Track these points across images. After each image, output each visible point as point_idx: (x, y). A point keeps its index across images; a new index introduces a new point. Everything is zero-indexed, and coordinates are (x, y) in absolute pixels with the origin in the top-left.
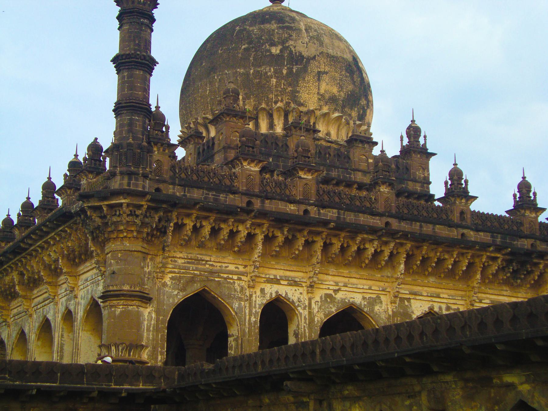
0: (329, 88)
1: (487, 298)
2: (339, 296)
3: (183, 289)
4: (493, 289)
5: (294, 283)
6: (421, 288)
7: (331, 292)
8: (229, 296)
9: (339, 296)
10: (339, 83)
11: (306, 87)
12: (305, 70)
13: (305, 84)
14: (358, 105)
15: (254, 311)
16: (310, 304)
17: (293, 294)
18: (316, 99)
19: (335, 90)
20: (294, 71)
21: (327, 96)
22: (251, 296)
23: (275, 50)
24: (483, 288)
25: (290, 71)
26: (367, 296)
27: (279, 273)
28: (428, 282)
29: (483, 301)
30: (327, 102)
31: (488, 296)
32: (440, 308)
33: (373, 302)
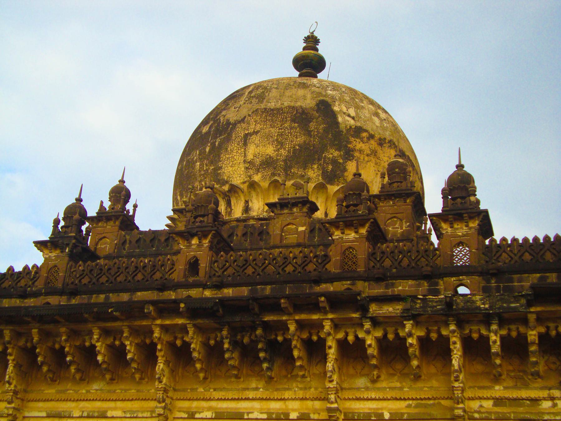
1: (209, 409)
4: (221, 390)
6: (73, 404)
10: (277, 140)
11: (228, 158)
13: (227, 156)
14: (319, 160)
18: (243, 169)
20: (217, 144)
21: (258, 161)
24: (201, 390)
28: (88, 391)
29: (197, 416)
30: (259, 169)
31: (213, 404)
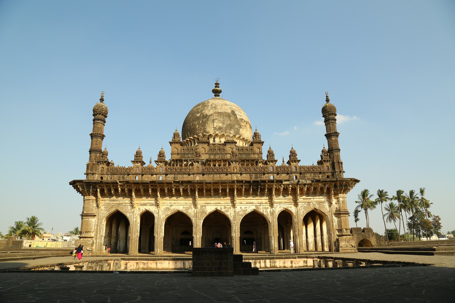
0: (218, 124)
2: (172, 208)
3: (108, 211)
5: (151, 205)
7: (169, 206)
8: (126, 212)
9: (172, 208)
12: (208, 119)
15: (135, 216)
16: (159, 212)
17: (152, 209)
19: (221, 125)
22: (134, 211)
23: (198, 115)
25: (203, 121)
26: (185, 206)
27: (146, 202)
32: (221, 208)
33: (187, 209)
